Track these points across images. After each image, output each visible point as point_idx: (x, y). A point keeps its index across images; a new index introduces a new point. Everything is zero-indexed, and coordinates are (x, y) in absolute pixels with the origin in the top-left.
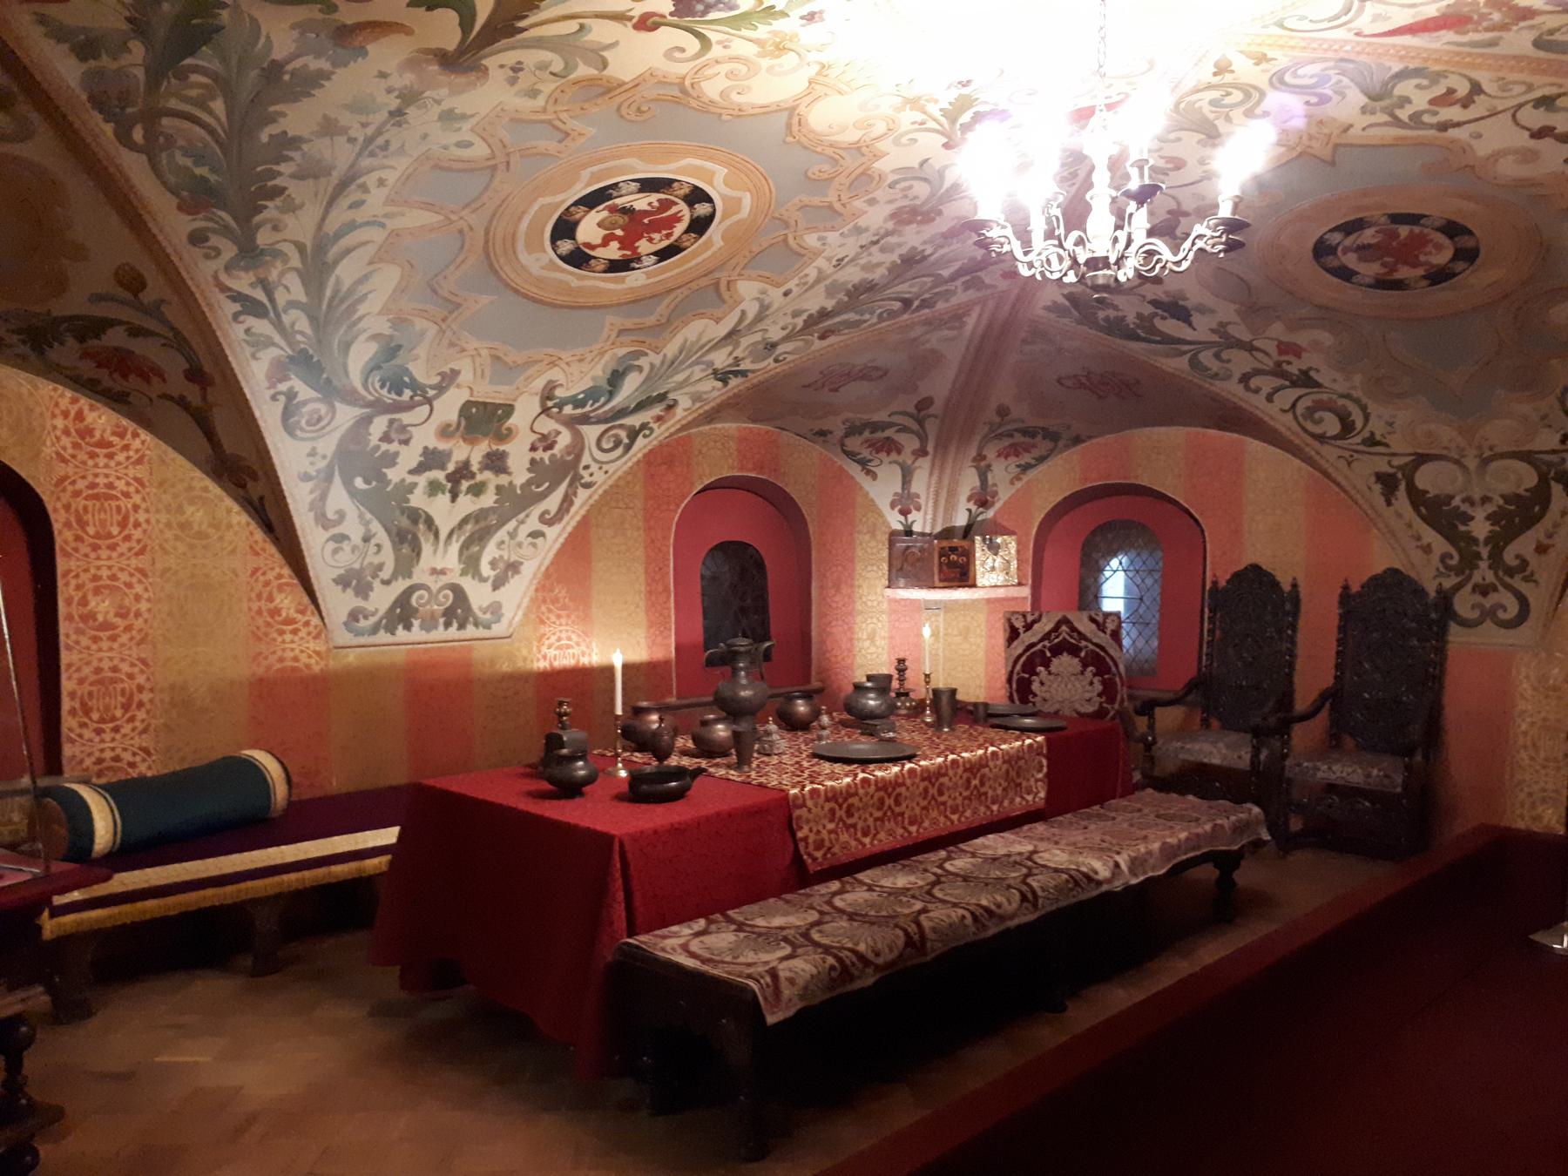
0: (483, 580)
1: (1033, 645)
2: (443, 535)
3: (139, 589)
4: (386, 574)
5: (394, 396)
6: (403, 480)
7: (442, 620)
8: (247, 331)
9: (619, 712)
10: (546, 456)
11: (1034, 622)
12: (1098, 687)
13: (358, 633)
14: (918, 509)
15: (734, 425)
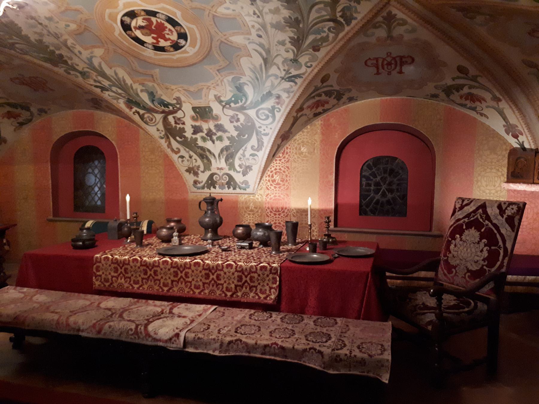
0: (239, 172)
1: (459, 220)
2: (217, 156)
3: (287, 173)
4: (202, 168)
6: (192, 137)
7: (226, 186)
9: (128, 218)
10: (239, 124)
11: (467, 205)
12: (485, 254)
13: (198, 188)
14: (522, 134)
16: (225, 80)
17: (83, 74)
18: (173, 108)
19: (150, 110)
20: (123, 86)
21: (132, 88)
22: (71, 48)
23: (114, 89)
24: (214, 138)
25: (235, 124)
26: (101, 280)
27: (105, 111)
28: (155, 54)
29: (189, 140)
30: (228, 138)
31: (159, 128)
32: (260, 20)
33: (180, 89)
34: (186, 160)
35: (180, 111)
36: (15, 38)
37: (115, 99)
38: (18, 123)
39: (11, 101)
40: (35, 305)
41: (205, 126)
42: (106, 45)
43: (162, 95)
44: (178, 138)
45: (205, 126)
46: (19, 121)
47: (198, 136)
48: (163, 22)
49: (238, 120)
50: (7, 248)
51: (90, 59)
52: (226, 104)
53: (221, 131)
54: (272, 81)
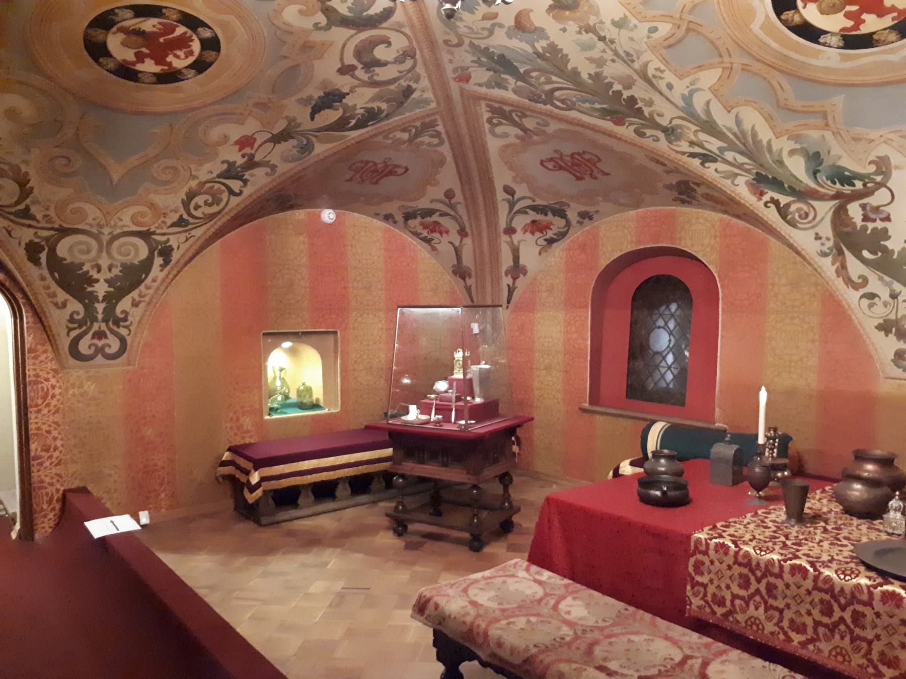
5: (847, 187)
8: (716, 170)
17: (671, 132)
18: (865, 185)
19: (804, 195)
20: (749, 147)
21: (770, 150)
22: (654, 81)
23: (729, 155)
26: (705, 595)
27: (702, 206)
28: (844, 58)
29: (895, 257)
31: (821, 234)
33: (891, 136)
34: (880, 304)
35: (884, 190)
36: (554, 78)
38: (545, 240)
39: (539, 202)
40: (566, 630)
42: (726, 59)
43: (840, 158)
44: (866, 254)
46: (547, 237)
50: (515, 448)
51: (688, 99)
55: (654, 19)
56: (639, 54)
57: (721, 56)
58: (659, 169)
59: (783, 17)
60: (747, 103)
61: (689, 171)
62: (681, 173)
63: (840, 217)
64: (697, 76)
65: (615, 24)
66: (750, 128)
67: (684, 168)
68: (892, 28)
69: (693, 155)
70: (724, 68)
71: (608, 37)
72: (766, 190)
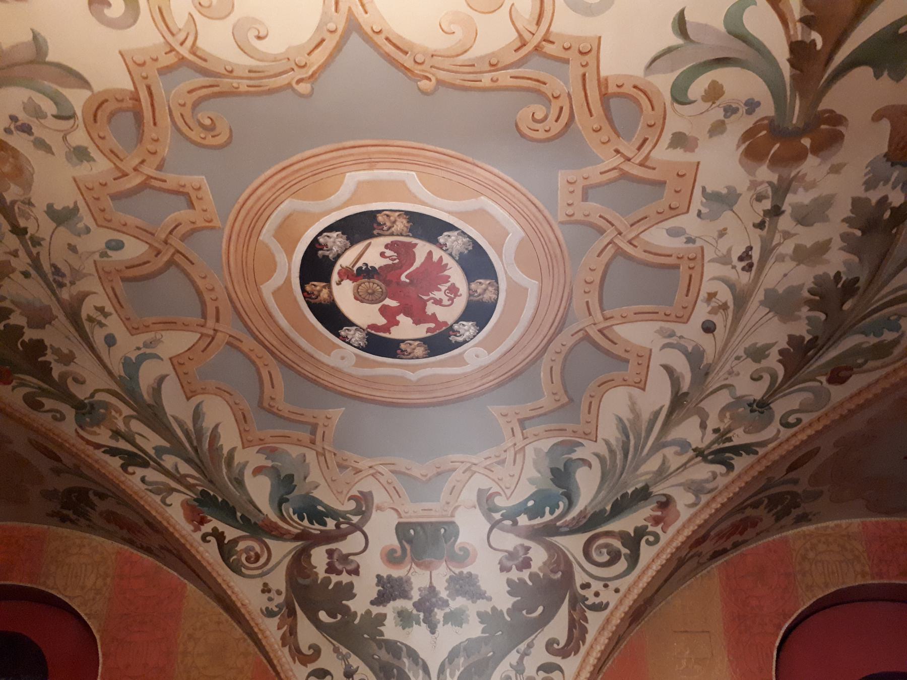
5: (317, 526)
6: (368, 612)
8: (143, 480)
15: (857, 521)
16: (530, 450)
17: (88, 412)
18: (337, 526)
19: (259, 529)
20: (201, 451)
22: (87, 326)
23: (169, 461)
24: (439, 614)
25: (515, 575)
30: (480, 615)
31: (271, 585)
32: (745, 278)
35: (358, 534)
37: (157, 492)
41: (419, 580)
44: (323, 616)
45: (419, 580)
47: (389, 610)
48: (447, 259)
49: (526, 564)
51: (132, 366)
52: (504, 517)
53: (464, 594)
54: (664, 457)
55: (123, 228)
56: (77, 275)
57: (204, 316)
58: (43, 465)
59: (308, 288)
60: (220, 391)
61: (104, 476)
62: (82, 475)
63: (299, 565)
64: (158, 336)
65: (51, 211)
66: (212, 426)
67: (90, 467)
68: (424, 341)
69: (113, 452)
70: (202, 335)
71: (31, 231)
72: (209, 518)
